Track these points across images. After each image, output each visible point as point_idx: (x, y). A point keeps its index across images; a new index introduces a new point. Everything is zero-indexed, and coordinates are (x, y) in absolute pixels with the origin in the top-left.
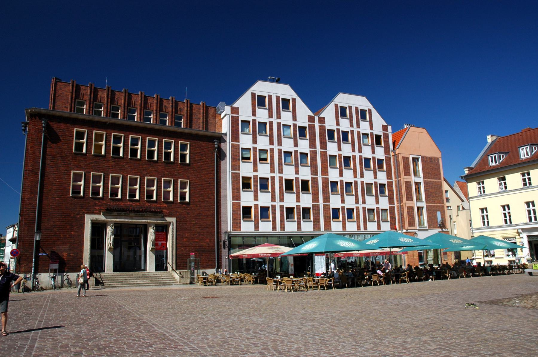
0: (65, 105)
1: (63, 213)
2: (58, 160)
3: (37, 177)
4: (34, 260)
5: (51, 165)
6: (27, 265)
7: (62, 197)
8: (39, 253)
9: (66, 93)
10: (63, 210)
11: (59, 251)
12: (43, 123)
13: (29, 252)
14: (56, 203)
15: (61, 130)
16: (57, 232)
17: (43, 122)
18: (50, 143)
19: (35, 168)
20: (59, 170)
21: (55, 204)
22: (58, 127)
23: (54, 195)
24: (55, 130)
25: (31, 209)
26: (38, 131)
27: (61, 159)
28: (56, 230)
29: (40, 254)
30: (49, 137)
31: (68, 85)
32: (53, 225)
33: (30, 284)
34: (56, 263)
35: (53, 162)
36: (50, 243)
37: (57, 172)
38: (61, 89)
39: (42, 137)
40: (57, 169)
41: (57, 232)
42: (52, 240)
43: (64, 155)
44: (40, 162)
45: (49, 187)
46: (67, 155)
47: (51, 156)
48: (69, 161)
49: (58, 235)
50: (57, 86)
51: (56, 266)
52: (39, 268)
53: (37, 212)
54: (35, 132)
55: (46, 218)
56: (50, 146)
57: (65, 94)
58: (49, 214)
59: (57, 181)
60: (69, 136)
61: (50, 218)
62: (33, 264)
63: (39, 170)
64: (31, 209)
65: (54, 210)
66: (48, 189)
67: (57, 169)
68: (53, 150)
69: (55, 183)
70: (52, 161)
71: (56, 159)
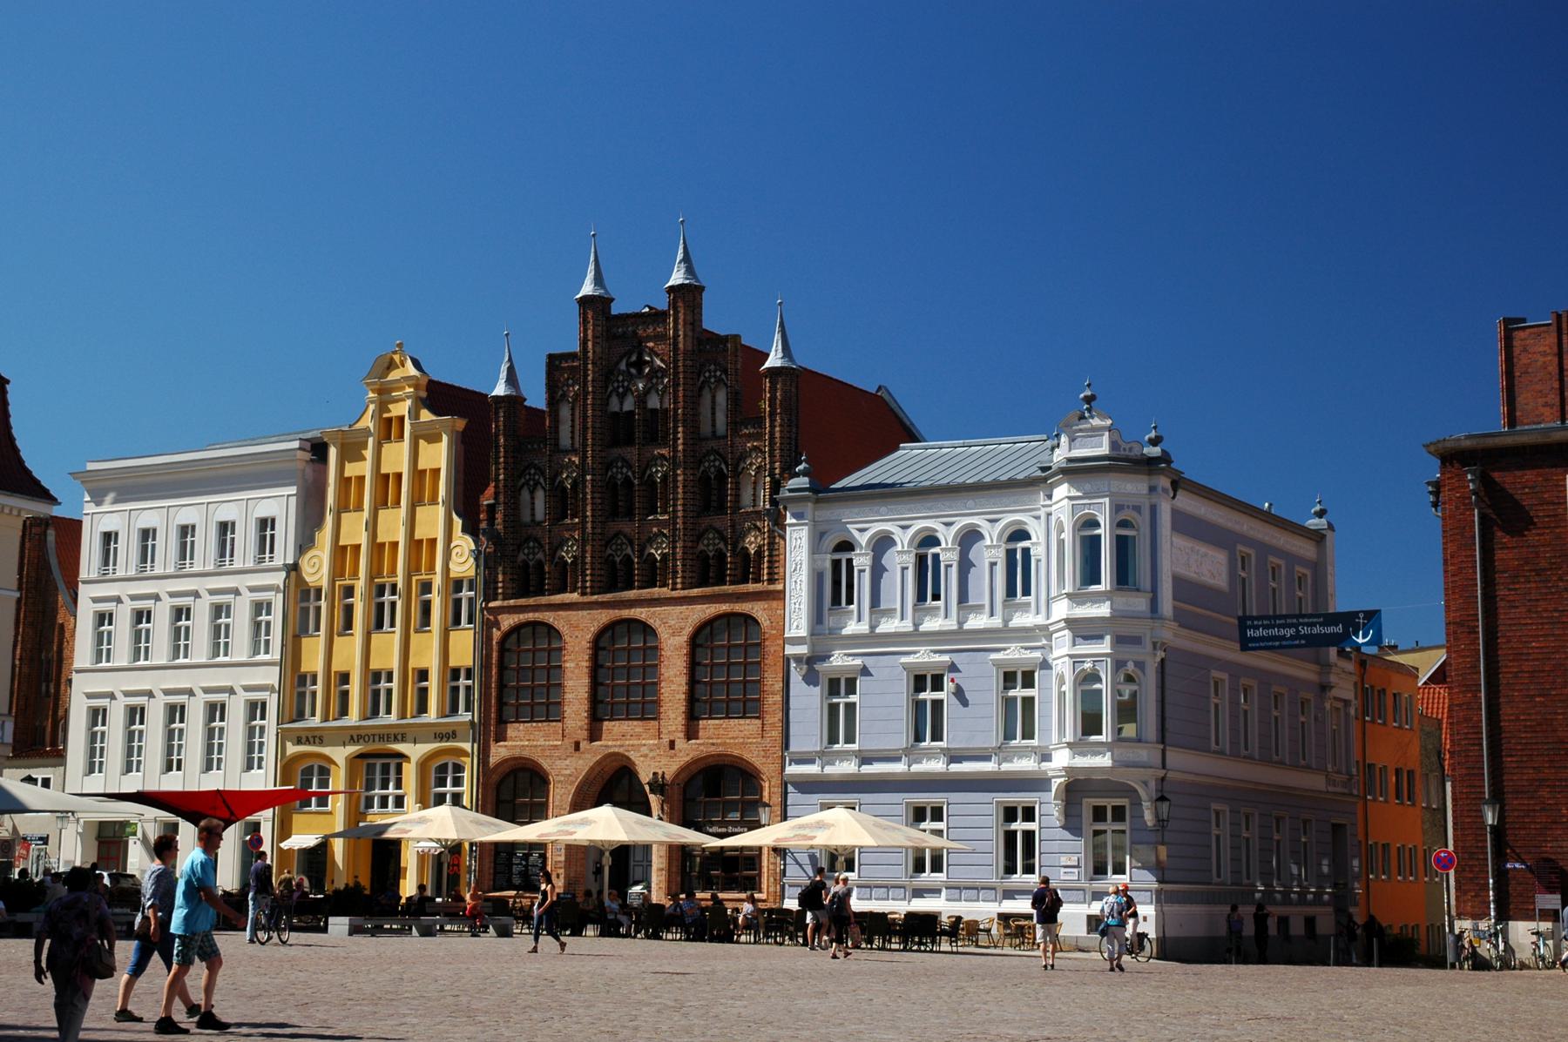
0: (1544, 400)
1: (1563, 742)
2: (1529, 582)
3: (1475, 642)
4: (1491, 881)
5: (1509, 601)
6: (1475, 896)
7: (1554, 693)
8: (1507, 861)
9: (1542, 359)
10: (1560, 734)
11: (1560, 857)
12: (1471, 481)
13: (1478, 859)
14: (1536, 714)
15: (1527, 490)
16: (1549, 799)
17: (1469, 477)
18: (1499, 534)
19: (1468, 615)
20: (1537, 612)
21: (1533, 717)
22: (1518, 481)
23: (1528, 690)
24: (1510, 491)
25: (1470, 736)
26: (1464, 504)
27: (1537, 579)
28: (1544, 793)
29: (1509, 866)
30: (1495, 517)
31: (1544, 332)
32: (1536, 780)
33: (1485, 949)
34: (1554, 893)
35: (1515, 589)
36: (1533, 832)
37: (1530, 618)
38: (1525, 350)
39: (1474, 522)
40: (1529, 611)
41: (1549, 799)
42: (1538, 823)
43: (1543, 564)
44: (1477, 597)
45: (1510, 667)
46: (1554, 563)
47: (1506, 572)
48: (1561, 579)
49: (1553, 807)
50: (1515, 343)
51: (1553, 902)
52: (1511, 907)
53: (1485, 743)
54: (1457, 508)
55: (1514, 759)
56: (1501, 543)
57: (1539, 364)
58: (1519, 747)
59: (1533, 648)
60: (1554, 504)
61: (1525, 759)
62: (1491, 893)
63: (1478, 620)
64: (1470, 736)
65: (1534, 735)
66: (1511, 673)
67: (1529, 611)
68: (1511, 556)
69: (1529, 654)
70: (1511, 587)
71: (1522, 580)
